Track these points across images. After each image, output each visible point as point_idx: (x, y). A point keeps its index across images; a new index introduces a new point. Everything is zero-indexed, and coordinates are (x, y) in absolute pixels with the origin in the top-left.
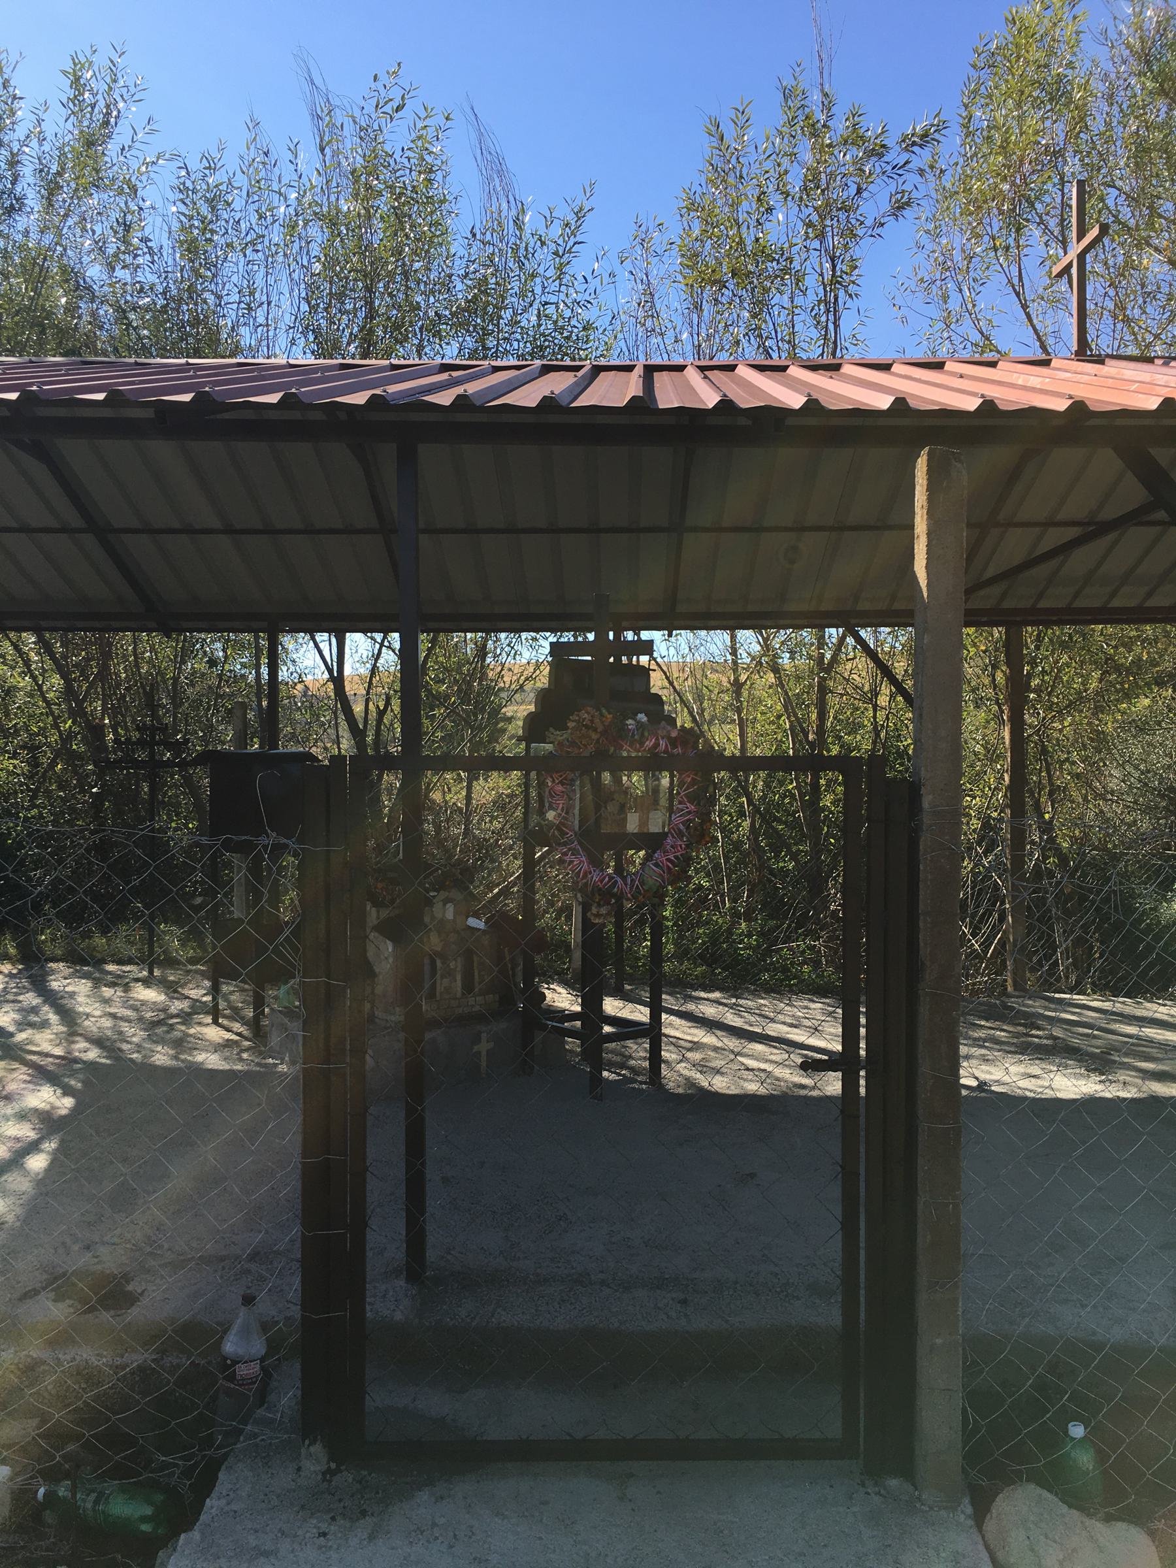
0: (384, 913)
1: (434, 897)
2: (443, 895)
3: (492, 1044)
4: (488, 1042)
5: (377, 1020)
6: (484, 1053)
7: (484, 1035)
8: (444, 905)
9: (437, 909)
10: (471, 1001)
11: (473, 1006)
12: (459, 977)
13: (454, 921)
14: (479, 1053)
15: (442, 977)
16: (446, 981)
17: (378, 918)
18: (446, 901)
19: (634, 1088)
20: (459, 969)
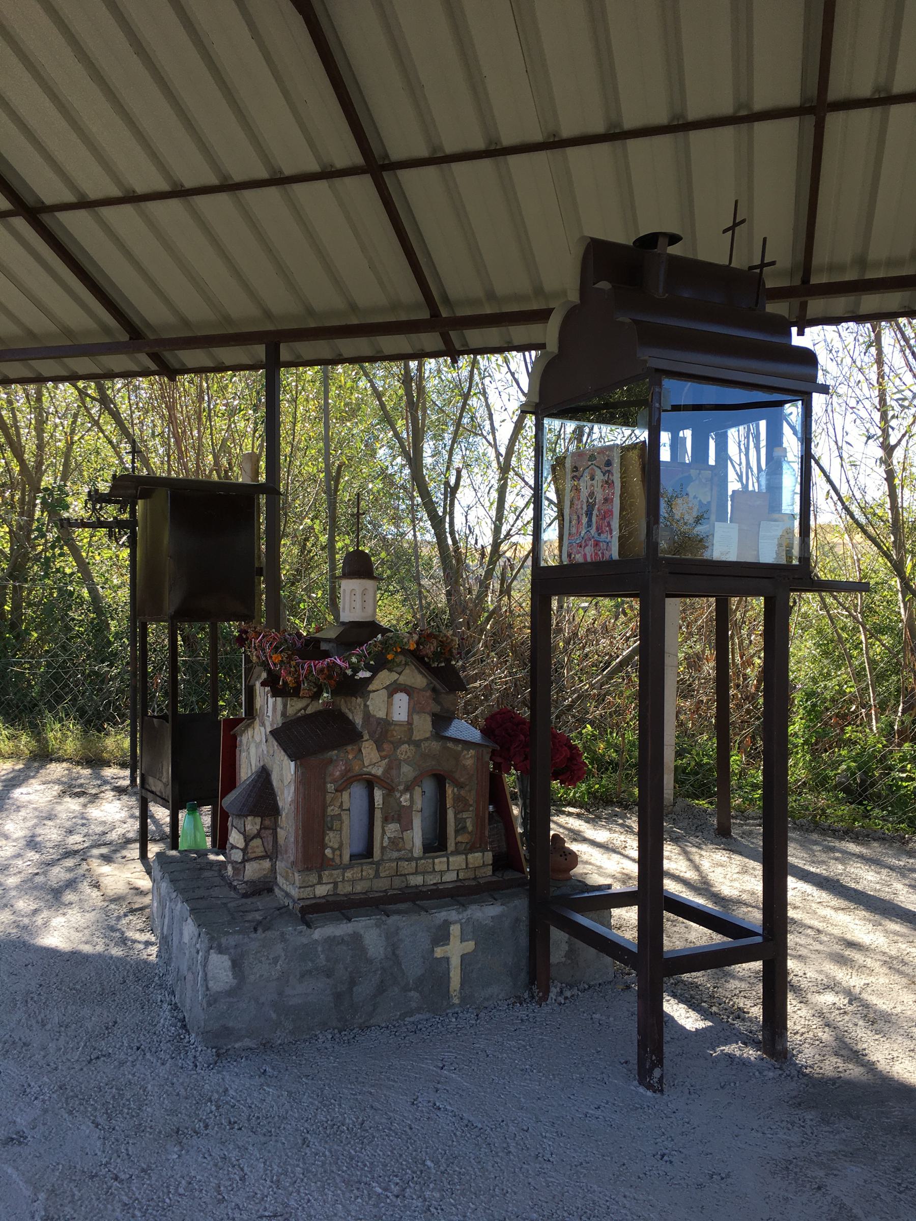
0: (296, 706)
1: (368, 681)
2: (385, 678)
3: (470, 946)
4: (462, 940)
5: (276, 890)
6: (455, 962)
7: (455, 930)
8: (391, 695)
9: (377, 704)
10: (440, 863)
11: (442, 873)
12: (417, 823)
13: (410, 723)
14: (447, 960)
15: (386, 820)
16: (393, 829)
17: (284, 714)
18: (394, 688)
19: (730, 1057)
20: (418, 805)
